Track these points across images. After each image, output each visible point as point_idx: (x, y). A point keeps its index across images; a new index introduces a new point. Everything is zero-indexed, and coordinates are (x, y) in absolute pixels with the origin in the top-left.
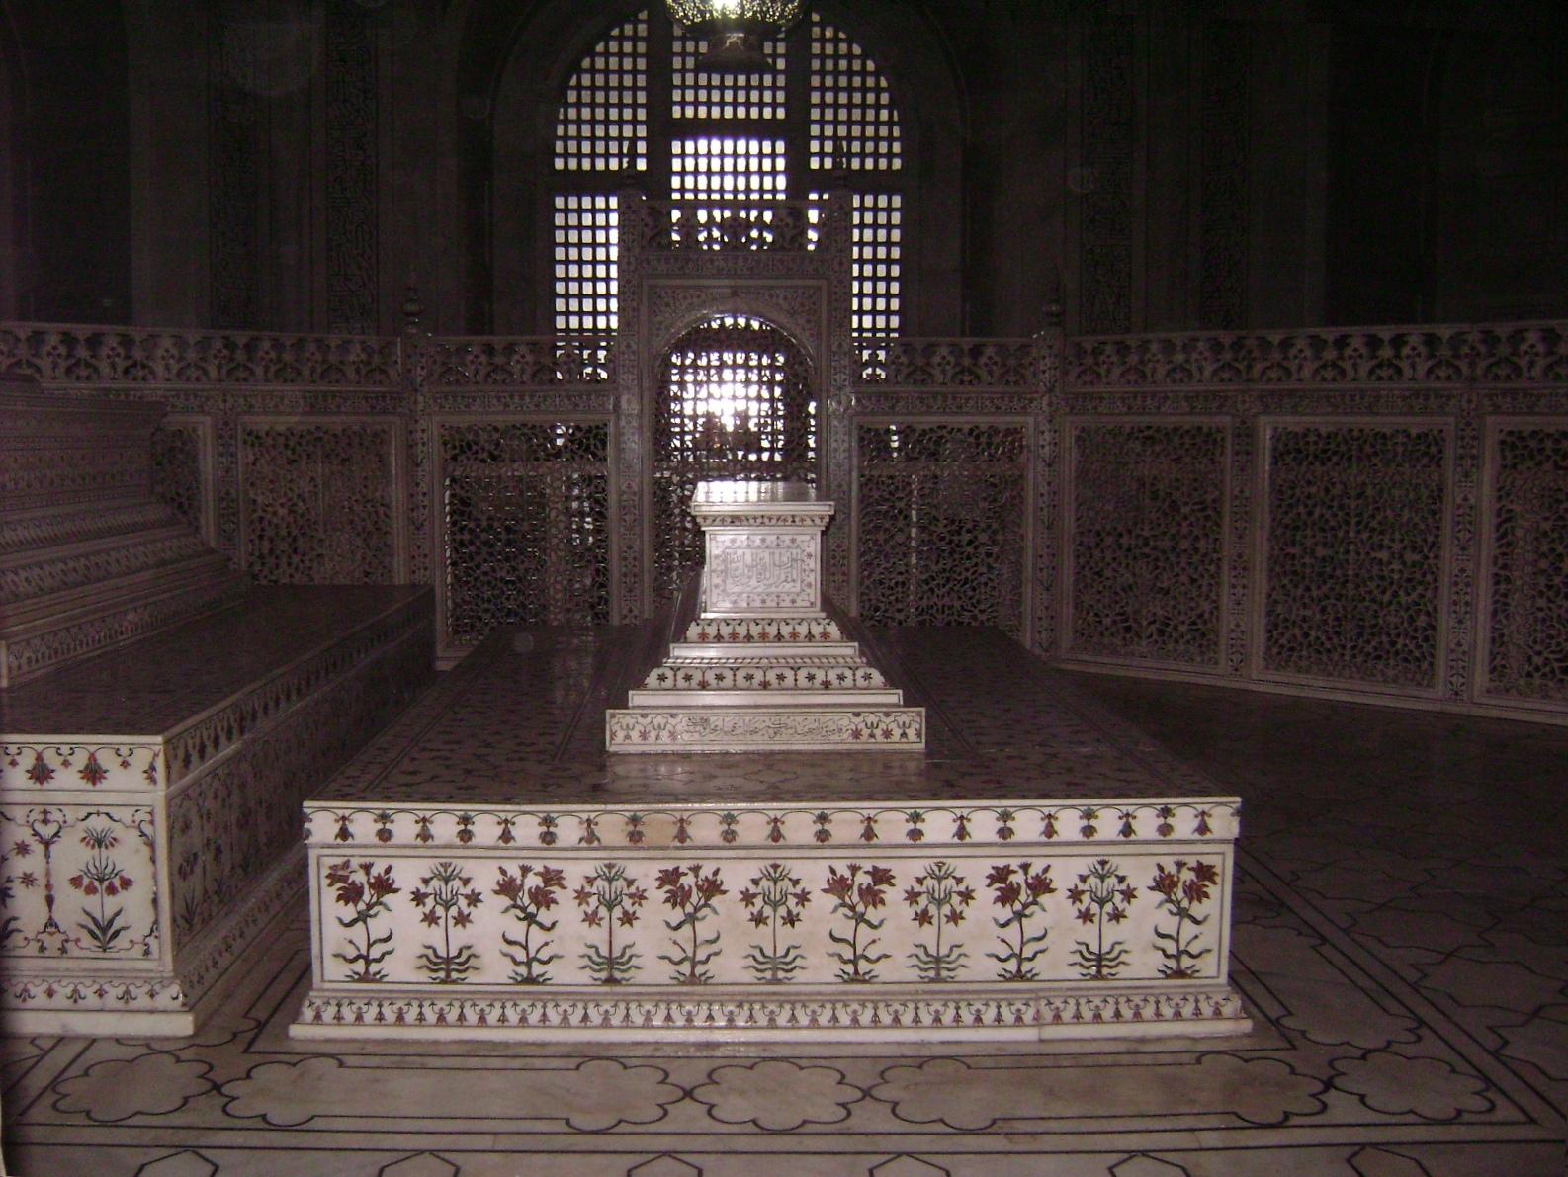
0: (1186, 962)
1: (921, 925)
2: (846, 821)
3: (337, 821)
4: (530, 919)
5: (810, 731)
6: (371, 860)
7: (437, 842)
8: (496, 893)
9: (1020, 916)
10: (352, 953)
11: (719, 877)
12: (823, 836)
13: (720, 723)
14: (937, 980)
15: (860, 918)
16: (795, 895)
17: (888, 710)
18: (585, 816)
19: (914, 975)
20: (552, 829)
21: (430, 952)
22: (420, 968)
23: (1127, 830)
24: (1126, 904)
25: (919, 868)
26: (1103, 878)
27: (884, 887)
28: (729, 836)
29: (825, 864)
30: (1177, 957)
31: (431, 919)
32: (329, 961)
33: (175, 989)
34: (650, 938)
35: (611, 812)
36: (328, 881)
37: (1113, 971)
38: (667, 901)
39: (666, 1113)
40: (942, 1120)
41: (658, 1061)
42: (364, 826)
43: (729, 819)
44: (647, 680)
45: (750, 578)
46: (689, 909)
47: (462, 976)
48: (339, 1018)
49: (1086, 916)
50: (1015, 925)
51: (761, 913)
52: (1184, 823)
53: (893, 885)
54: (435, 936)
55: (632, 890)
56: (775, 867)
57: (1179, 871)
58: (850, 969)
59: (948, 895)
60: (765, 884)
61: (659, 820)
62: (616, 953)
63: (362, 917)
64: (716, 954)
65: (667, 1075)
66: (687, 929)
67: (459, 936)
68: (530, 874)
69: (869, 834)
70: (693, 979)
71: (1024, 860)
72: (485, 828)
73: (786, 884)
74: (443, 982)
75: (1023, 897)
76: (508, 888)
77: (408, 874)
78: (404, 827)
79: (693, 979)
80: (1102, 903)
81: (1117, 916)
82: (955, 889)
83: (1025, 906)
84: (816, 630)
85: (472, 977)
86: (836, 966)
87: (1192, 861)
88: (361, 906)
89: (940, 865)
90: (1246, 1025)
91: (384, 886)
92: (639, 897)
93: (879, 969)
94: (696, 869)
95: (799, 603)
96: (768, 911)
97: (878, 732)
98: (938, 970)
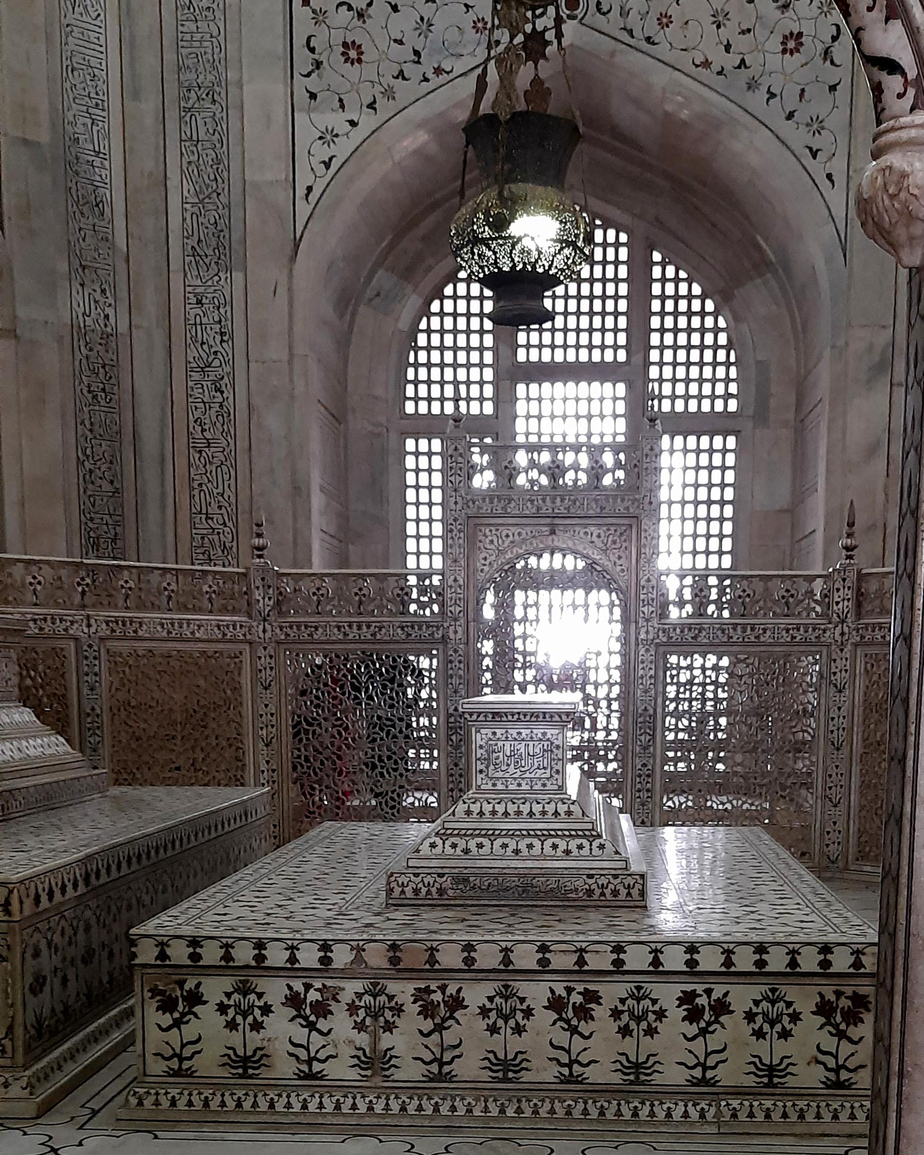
0: (844, 1075)
4: (312, 1026)
15: (574, 1031)
19: (617, 1078)
20: (329, 954)
24: (792, 1025)
25: (622, 990)
31: (232, 1025)
49: (759, 1034)
53: (600, 1004)
54: (235, 1038)
55: (393, 1004)
56: (506, 987)
57: (838, 999)
58: (566, 1071)
59: (646, 1012)
63: (177, 1023)
64: (459, 1057)
66: (435, 1037)
67: (255, 1039)
68: (312, 991)
70: (441, 1077)
71: (708, 986)
74: (241, 1076)
75: (706, 1017)
80: (772, 1024)
81: (785, 1034)
83: (709, 1024)
85: (263, 1072)
86: (555, 1069)
87: (849, 991)
88: (176, 1015)
89: (639, 988)
91: (195, 998)
93: (588, 1072)
94: (443, 988)
98: (637, 1075)
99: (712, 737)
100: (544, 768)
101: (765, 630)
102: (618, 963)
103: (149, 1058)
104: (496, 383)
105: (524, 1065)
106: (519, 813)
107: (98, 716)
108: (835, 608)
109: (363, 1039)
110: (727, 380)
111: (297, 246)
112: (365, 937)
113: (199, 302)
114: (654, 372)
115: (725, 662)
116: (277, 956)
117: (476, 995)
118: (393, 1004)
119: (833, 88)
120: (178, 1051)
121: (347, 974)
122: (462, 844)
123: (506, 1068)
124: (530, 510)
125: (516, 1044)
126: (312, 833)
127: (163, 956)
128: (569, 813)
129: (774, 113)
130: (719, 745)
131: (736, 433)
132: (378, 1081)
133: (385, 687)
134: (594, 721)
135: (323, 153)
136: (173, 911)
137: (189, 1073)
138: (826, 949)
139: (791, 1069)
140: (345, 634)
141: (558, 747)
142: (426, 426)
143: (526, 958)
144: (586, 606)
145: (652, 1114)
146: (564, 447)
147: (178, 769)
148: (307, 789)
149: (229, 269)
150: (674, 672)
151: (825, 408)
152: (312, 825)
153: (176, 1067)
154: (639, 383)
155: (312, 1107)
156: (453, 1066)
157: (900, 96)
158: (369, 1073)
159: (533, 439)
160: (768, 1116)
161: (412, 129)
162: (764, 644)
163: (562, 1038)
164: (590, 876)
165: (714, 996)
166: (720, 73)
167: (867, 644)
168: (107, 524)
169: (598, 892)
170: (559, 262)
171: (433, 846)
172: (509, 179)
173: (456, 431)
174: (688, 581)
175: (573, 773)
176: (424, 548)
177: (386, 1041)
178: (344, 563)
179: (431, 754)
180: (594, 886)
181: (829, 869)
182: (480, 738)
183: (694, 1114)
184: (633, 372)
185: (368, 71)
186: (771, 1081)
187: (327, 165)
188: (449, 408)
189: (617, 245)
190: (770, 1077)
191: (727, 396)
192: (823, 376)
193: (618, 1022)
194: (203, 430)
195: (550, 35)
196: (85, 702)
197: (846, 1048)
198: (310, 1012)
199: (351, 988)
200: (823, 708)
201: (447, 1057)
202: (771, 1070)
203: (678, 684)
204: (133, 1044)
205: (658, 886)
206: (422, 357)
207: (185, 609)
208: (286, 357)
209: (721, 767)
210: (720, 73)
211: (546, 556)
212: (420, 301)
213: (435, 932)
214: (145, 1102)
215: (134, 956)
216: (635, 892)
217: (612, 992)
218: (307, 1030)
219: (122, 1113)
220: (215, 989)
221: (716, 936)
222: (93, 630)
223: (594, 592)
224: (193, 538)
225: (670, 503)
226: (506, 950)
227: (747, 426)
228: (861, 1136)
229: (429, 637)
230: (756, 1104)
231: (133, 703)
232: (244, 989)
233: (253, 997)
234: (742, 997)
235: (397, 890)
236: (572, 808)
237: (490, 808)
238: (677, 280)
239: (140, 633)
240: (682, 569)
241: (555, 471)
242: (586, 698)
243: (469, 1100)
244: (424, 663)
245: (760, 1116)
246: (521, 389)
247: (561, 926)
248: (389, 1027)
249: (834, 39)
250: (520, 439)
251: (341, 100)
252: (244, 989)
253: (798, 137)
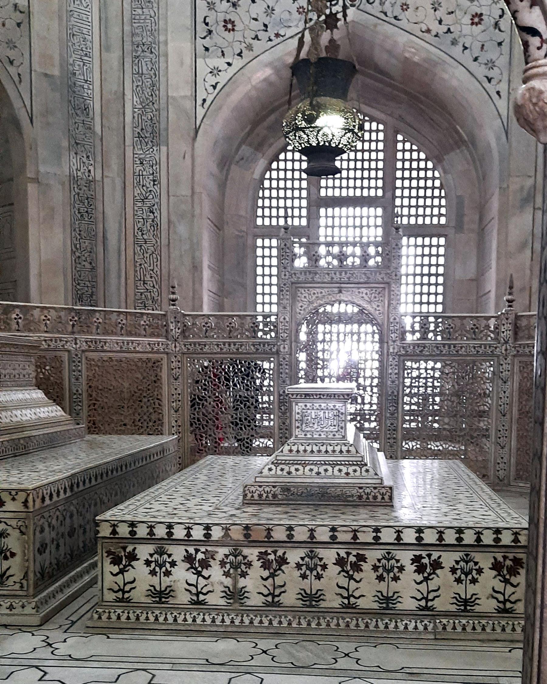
0: (508, 605)
4: (199, 574)
7: (156, 537)
9: (426, 579)
10: (116, 588)
11: (285, 556)
15: (351, 578)
19: (376, 606)
20: (209, 532)
31: (153, 573)
46: (272, 571)
49: (458, 581)
50: (425, 583)
53: (366, 562)
54: (155, 581)
55: (246, 561)
56: (312, 552)
57: (505, 560)
58: (346, 601)
59: (392, 567)
60: (307, 559)
63: (122, 572)
64: (284, 592)
66: (270, 580)
68: (199, 553)
71: (428, 552)
74: (158, 603)
75: (428, 570)
80: (466, 575)
81: (474, 581)
83: (430, 574)
85: (171, 600)
86: (339, 600)
87: (511, 556)
88: (121, 566)
89: (389, 553)
91: (132, 557)
94: (275, 552)
98: (387, 604)
99: (431, 408)
100: (334, 426)
101: (461, 347)
102: (377, 538)
103: (105, 591)
104: (308, 208)
105: (322, 597)
106: (319, 451)
107: (80, 394)
108: (502, 334)
109: (228, 582)
110: (440, 206)
111: (197, 131)
112: (230, 522)
113: (141, 163)
114: (398, 202)
115: (439, 365)
116: (179, 533)
117: (294, 556)
118: (246, 561)
119: (500, 44)
121: (220, 543)
122: (286, 468)
123: (311, 599)
124: (327, 279)
125: (317, 585)
126: (201, 462)
127: (114, 532)
128: (348, 451)
129: (467, 58)
130: (435, 413)
131: (445, 236)
132: (237, 606)
133: (243, 379)
134: (363, 399)
135: (212, 80)
136: (121, 507)
137: (128, 600)
138: (498, 531)
139: (477, 601)
140: (221, 349)
141: (342, 414)
142: (269, 232)
143: (323, 535)
144: (359, 334)
145: (396, 627)
146: (347, 244)
147: (125, 425)
148: (198, 437)
149: (158, 145)
150: (409, 371)
151: (495, 223)
152: (201, 458)
153: (121, 597)
154: (389, 209)
155: (199, 621)
156: (280, 598)
157: (539, 48)
158: (231, 601)
159: (329, 239)
160: (464, 629)
161: (262, 68)
162: (461, 355)
163: (344, 582)
164: (361, 488)
165: (433, 558)
166: (436, 36)
167: (520, 356)
168: (87, 287)
169: (365, 497)
170: (344, 141)
171: (270, 470)
172: (316, 94)
173: (286, 235)
174: (418, 319)
175: (351, 428)
176: (267, 301)
177: (242, 582)
178: (221, 309)
179: (270, 417)
180: (363, 494)
181: (499, 486)
182: (297, 408)
183: (421, 628)
184: (386, 202)
185: (238, 36)
186: (465, 608)
187: (214, 87)
188: (282, 222)
189: (377, 131)
190: (465, 606)
191: (440, 215)
192: (495, 204)
193: (377, 573)
194: (143, 234)
195: (340, 16)
196: (73, 387)
197: (510, 590)
198: (198, 566)
199: (222, 551)
200: (495, 392)
201: (277, 592)
202: (466, 602)
203: (412, 378)
204: (96, 583)
205: (400, 494)
206: (267, 193)
207: (130, 334)
208: (189, 193)
209: (436, 425)
210: (436, 36)
211: (336, 305)
212: (266, 162)
213: (271, 520)
214: (103, 617)
215: (98, 532)
216: (386, 497)
217: (373, 555)
218: (196, 576)
219: (90, 624)
220: (144, 551)
221: (434, 523)
222: (78, 346)
223: (364, 325)
224: (135, 295)
225: (407, 275)
226: (312, 530)
227: (451, 232)
228: (518, 641)
229: (269, 351)
230: (457, 621)
231: (100, 387)
232: (161, 552)
233: (165, 556)
234: (449, 559)
235: (249, 495)
236: (350, 448)
237: (303, 448)
238: (411, 151)
239: (105, 348)
240: (414, 313)
241: (342, 257)
242: (359, 386)
243: (289, 617)
244: (266, 365)
245: (459, 629)
246: (322, 211)
247: (343, 517)
248: (244, 575)
249: (501, 17)
250: (322, 239)
251: (222, 52)
252: (161, 552)
253: (480, 71)
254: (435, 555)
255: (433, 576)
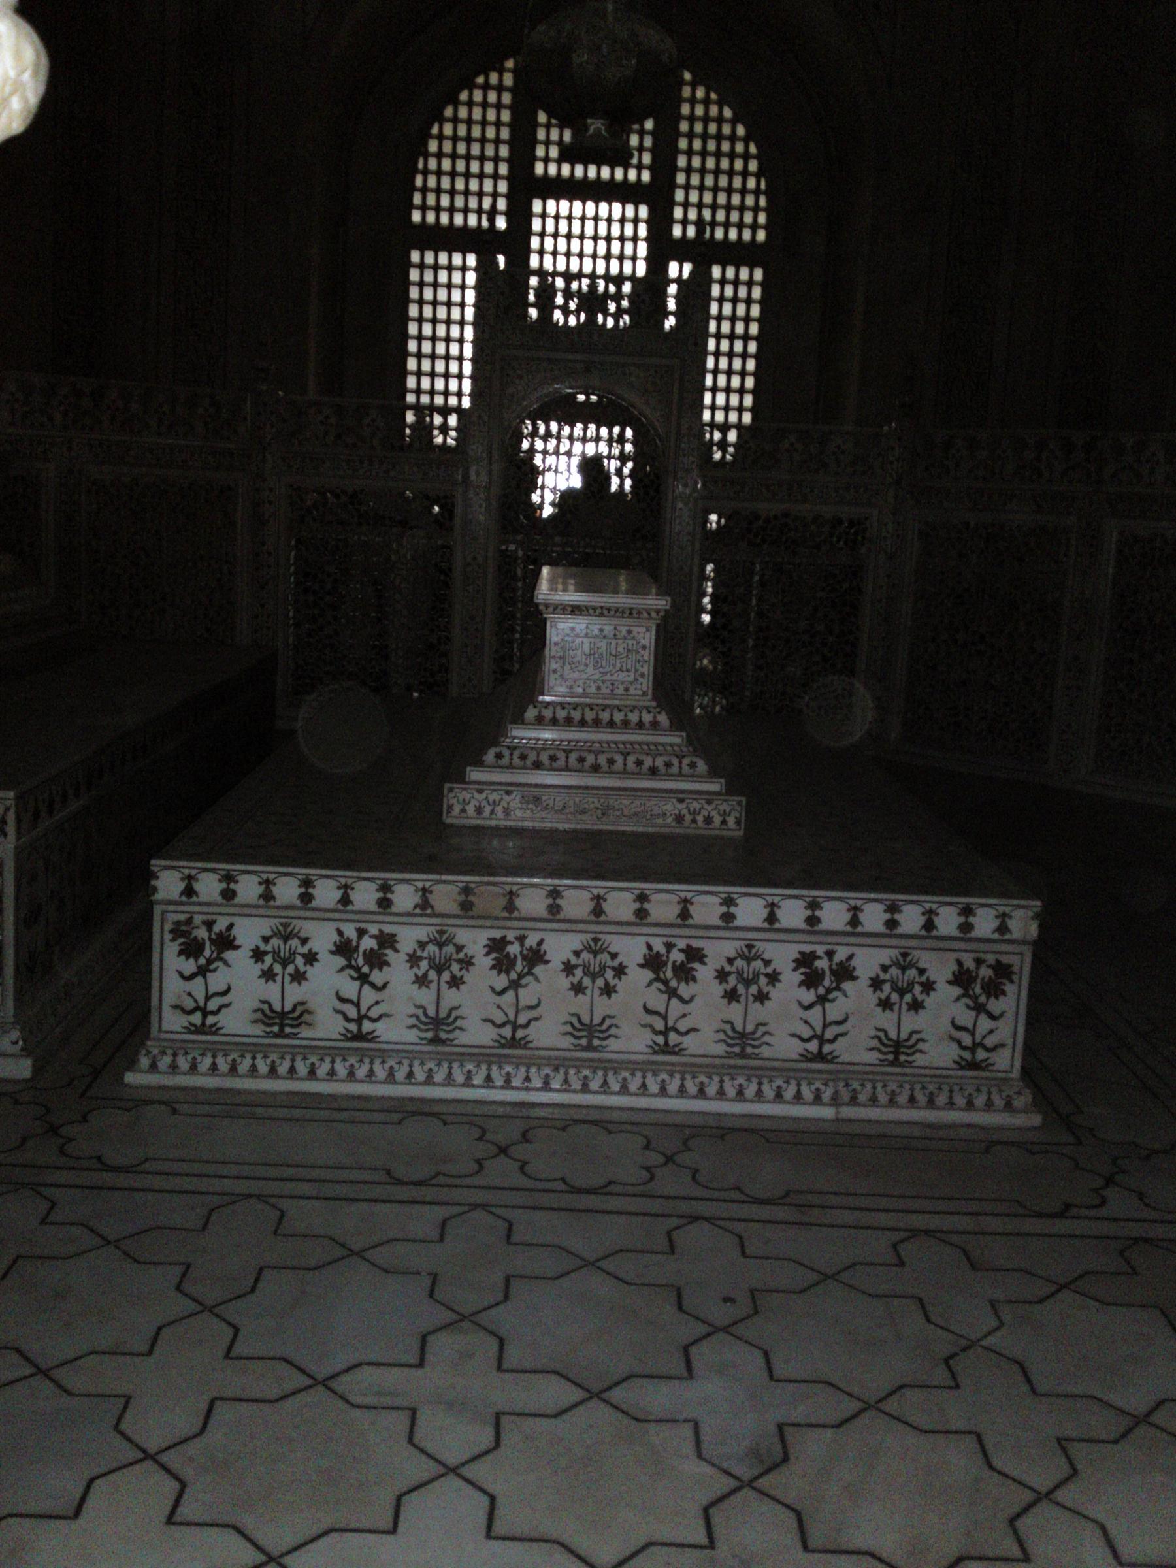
0: (981, 1055)
1: (729, 1003)
2: (664, 903)
3: (182, 879)
4: (364, 979)
5: (636, 814)
6: (214, 917)
7: (278, 903)
8: (332, 952)
9: (822, 1000)
12: (641, 914)
13: (551, 802)
14: (743, 1055)
15: (672, 993)
16: (613, 968)
17: (710, 797)
18: (420, 885)
19: (720, 1049)
21: (265, 1007)
22: (255, 1022)
23: (929, 926)
25: (729, 948)
26: (904, 969)
27: (696, 965)
28: (554, 909)
29: (643, 939)
30: (972, 1049)
31: (268, 975)
32: (167, 1013)
33: (15, 1034)
34: (477, 1004)
35: (444, 882)
36: (170, 936)
37: (910, 1059)
38: (493, 967)
39: (481, 1167)
40: (738, 1189)
41: (475, 1119)
42: (209, 886)
43: (555, 893)
44: (485, 758)
45: (586, 665)
47: (295, 1031)
48: (174, 1067)
49: (885, 1004)
50: (818, 1008)
51: (580, 982)
52: (984, 923)
53: (705, 964)
54: (272, 992)
55: (461, 955)
56: (596, 940)
58: (660, 1040)
59: (756, 975)
60: (585, 956)
61: (489, 891)
62: (442, 1014)
64: (536, 1019)
65: (484, 1131)
66: (510, 996)
68: (366, 937)
69: (685, 915)
70: (513, 1042)
71: (829, 947)
72: (326, 892)
73: (604, 957)
74: (276, 1036)
75: (827, 982)
76: (344, 948)
77: (249, 932)
78: (248, 888)
79: (513, 1042)
80: (902, 992)
81: (916, 1006)
82: (763, 970)
84: (647, 718)
85: (305, 1032)
86: (647, 1037)
87: (991, 959)
88: (202, 961)
90: (1036, 1120)
91: (225, 942)
92: (467, 963)
93: (688, 1042)
94: (521, 939)
95: (632, 691)
96: (587, 981)
97: (700, 818)
118: (461, 955)
120: (201, 1004)
125: (603, 1006)
190: (897, 1054)
197: (984, 1024)
218: (358, 983)
254: (841, 954)
255: (835, 994)
